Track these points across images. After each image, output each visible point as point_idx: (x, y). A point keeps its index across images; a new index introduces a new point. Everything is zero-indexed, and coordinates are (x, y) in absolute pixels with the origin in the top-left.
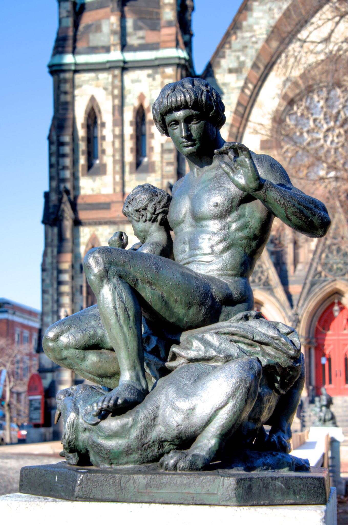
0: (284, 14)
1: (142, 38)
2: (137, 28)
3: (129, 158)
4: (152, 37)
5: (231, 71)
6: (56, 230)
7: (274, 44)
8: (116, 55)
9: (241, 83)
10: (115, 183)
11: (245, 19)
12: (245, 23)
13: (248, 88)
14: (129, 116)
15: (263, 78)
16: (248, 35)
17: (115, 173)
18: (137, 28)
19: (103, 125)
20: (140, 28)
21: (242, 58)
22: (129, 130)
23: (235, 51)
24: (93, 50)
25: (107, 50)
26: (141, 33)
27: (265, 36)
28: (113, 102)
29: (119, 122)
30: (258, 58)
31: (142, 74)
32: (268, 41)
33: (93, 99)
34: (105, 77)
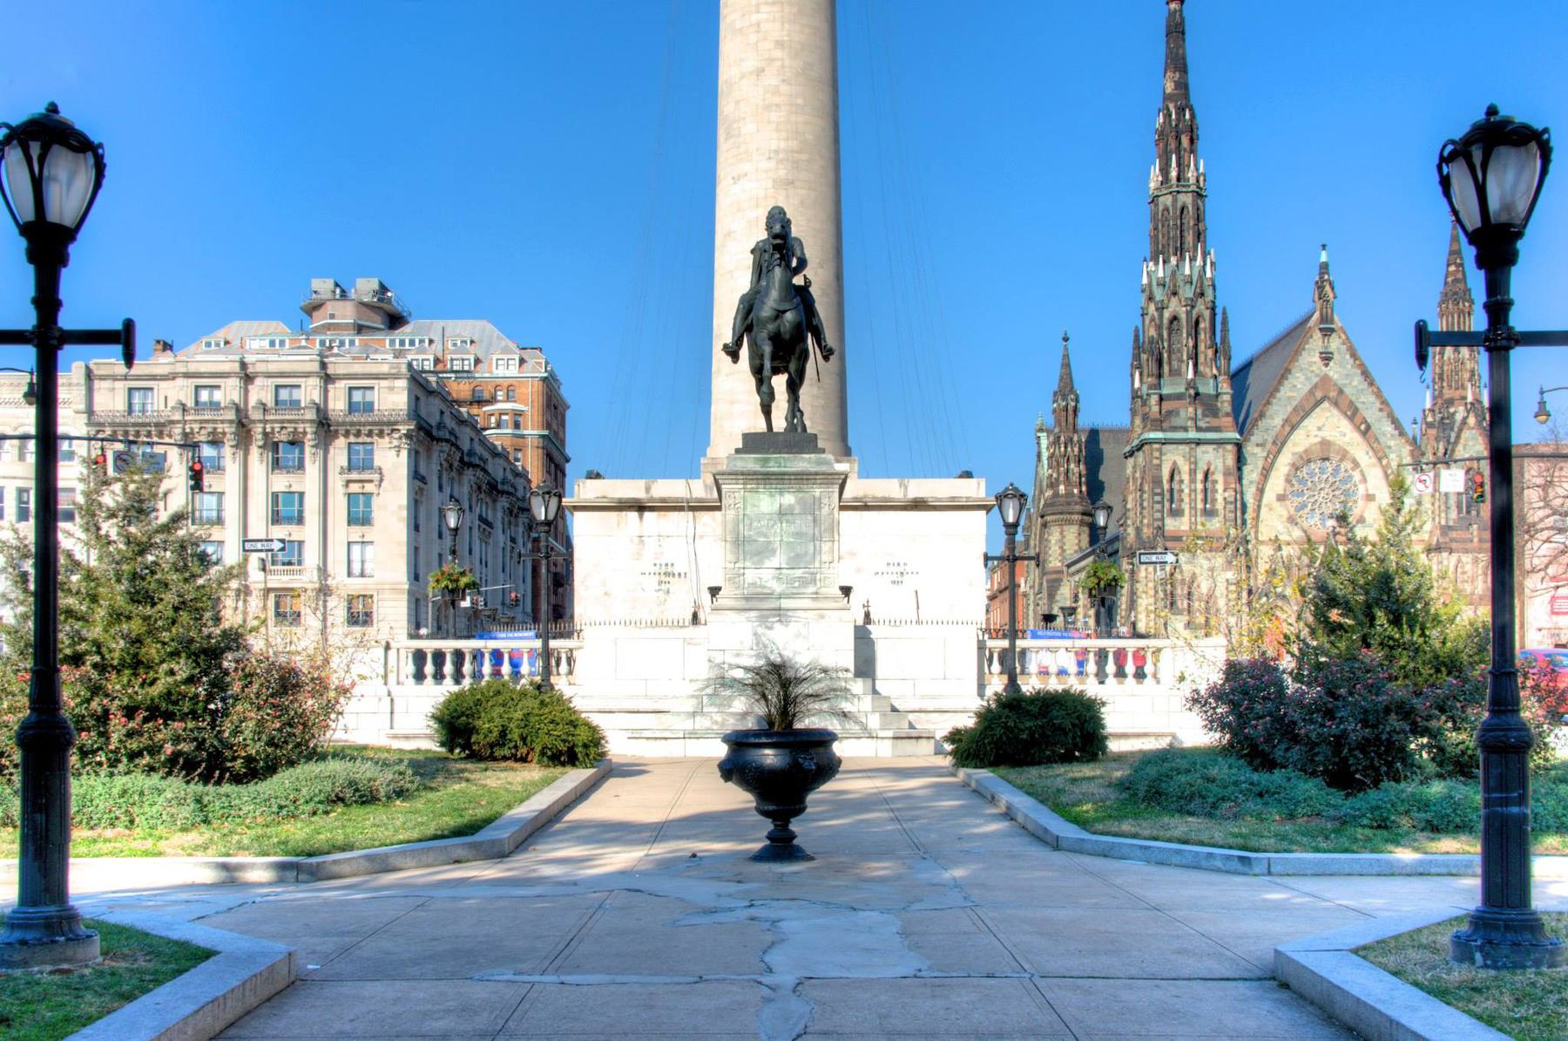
2: (1204, 415)
3: (1200, 505)
4: (1215, 422)
7: (1288, 429)
8: (1192, 434)
14: (1200, 476)
15: (1279, 452)
18: (1204, 415)
22: (1200, 486)
24: (1174, 429)
25: (1186, 429)
29: (1193, 481)
31: (1210, 448)
34: (1184, 448)
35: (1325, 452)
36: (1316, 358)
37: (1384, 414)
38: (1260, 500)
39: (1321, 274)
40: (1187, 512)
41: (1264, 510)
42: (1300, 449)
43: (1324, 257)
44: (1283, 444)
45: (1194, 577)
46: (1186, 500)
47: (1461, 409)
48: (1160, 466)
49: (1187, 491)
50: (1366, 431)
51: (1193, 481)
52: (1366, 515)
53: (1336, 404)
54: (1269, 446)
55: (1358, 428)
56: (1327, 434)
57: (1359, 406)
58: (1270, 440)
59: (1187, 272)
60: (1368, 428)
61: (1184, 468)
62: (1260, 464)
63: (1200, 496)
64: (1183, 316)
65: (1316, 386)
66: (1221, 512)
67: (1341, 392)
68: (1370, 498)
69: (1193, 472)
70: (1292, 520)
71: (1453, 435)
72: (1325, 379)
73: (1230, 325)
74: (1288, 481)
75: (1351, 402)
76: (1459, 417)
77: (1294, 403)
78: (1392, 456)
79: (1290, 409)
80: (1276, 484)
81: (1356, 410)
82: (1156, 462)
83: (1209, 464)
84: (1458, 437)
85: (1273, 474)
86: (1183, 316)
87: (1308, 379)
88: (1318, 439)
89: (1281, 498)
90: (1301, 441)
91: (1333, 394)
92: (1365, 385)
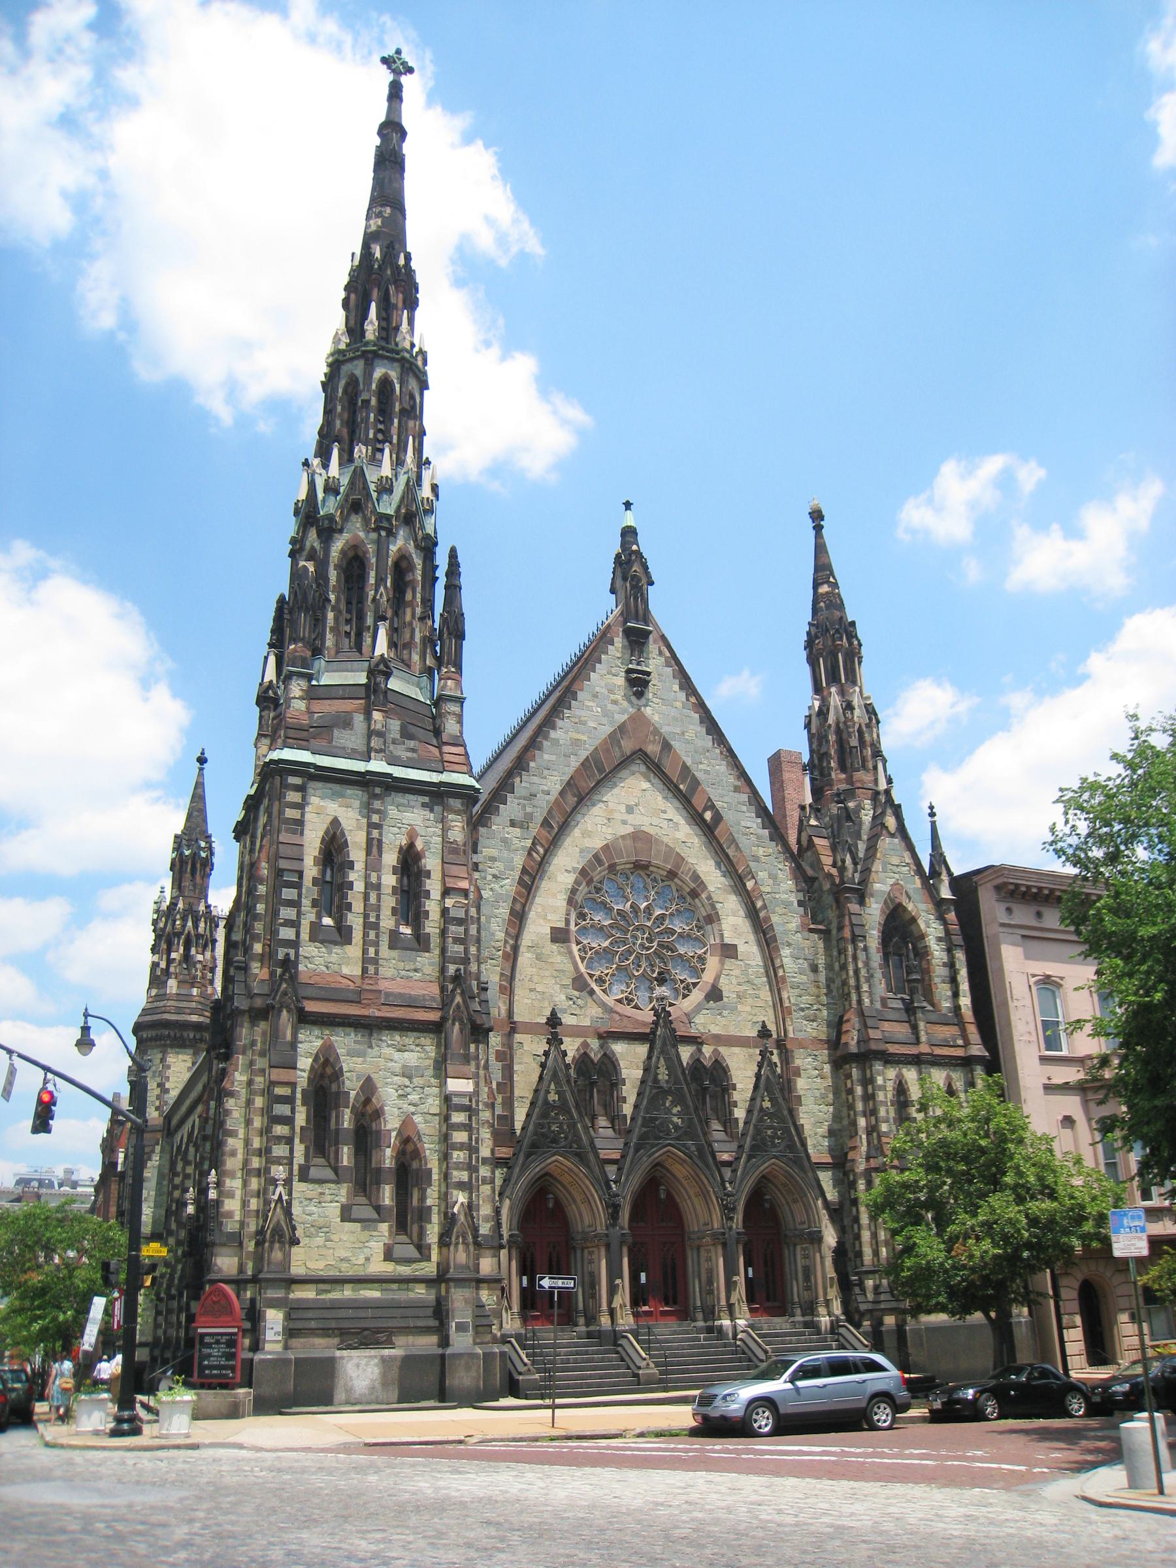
0: (582, 764)
1: (413, 750)
5: (513, 824)
6: (263, 1025)
7: (572, 800)
8: (378, 765)
9: (529, 843)
10: (365, 960)
11: (533, 759)
12: (532, 764)
13: (537, 853)
16: (536, 779)
17: (366, 943)
19: (351, 865)
20: (411, 737)
21: (529, 810)
22: (389, 880)
23: (520, 798)
26: (412, 744)
27: (559, 788)
28: (368, 833)
29: (374, 864)
30: (550, 812)
32: (562, 793)
33: (335, 822)
35: (632, 867)
36: (620, 681)
37: (744, 797)
38: (517, 937)
39: (624, 545)
40: (357, 935)
41: (525, 958)
42: (597, 843)
43: (629, 519)
44: (565, 827)
45: (369, 1087)
46: (358, 906)
47: (867, 803)
48: (300, 823)
49: (359, 886)
50: (709, 827)
51: (374, 864)
52: (723, 983)
53: (655, 769)
54: (535, 828)
55: (696, 818)
56: (643, 821)
57: (699, 775)
58: (539, 818)
59: (386, 470)
60: (718, 817)
61: (356, 839)
62: (519, 860)
63: (389, 902)
64: (371, 548)
65: (622, 728)
66: (435, 941)
67: (667, 746)
68: (729, 951)
69: (374, 847)
70: (579, 983)
71: (862, 846)
72: (638, 719)
73: (464, 580)
74: (570, 901)
75: (685, 768)
76: (867, 816)
77: (584, 754)
78: (762, 875)
79: (575, 763)
80: (551, 905)
81: (695, 783)
82: (290, 813)
83: (412, 835)
84: (872, 848)
85: (545, 885)
86: (371, 548)
87: (606, 713)
88: (629, 829)
89: (559, 936)
90: (599, 827)
91: (653, 749)
92: (708, 741)
